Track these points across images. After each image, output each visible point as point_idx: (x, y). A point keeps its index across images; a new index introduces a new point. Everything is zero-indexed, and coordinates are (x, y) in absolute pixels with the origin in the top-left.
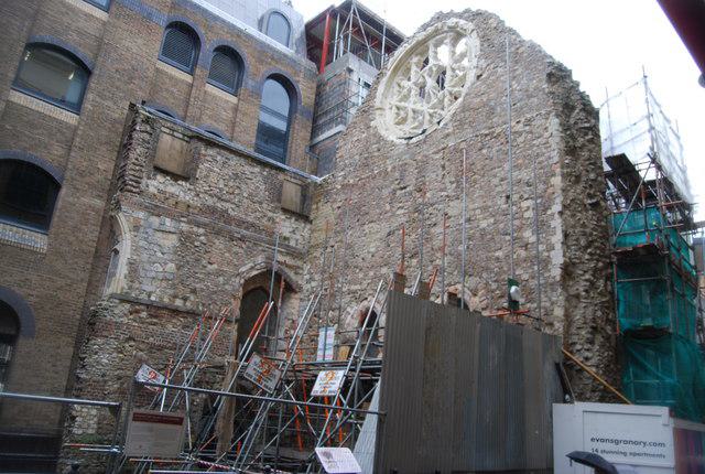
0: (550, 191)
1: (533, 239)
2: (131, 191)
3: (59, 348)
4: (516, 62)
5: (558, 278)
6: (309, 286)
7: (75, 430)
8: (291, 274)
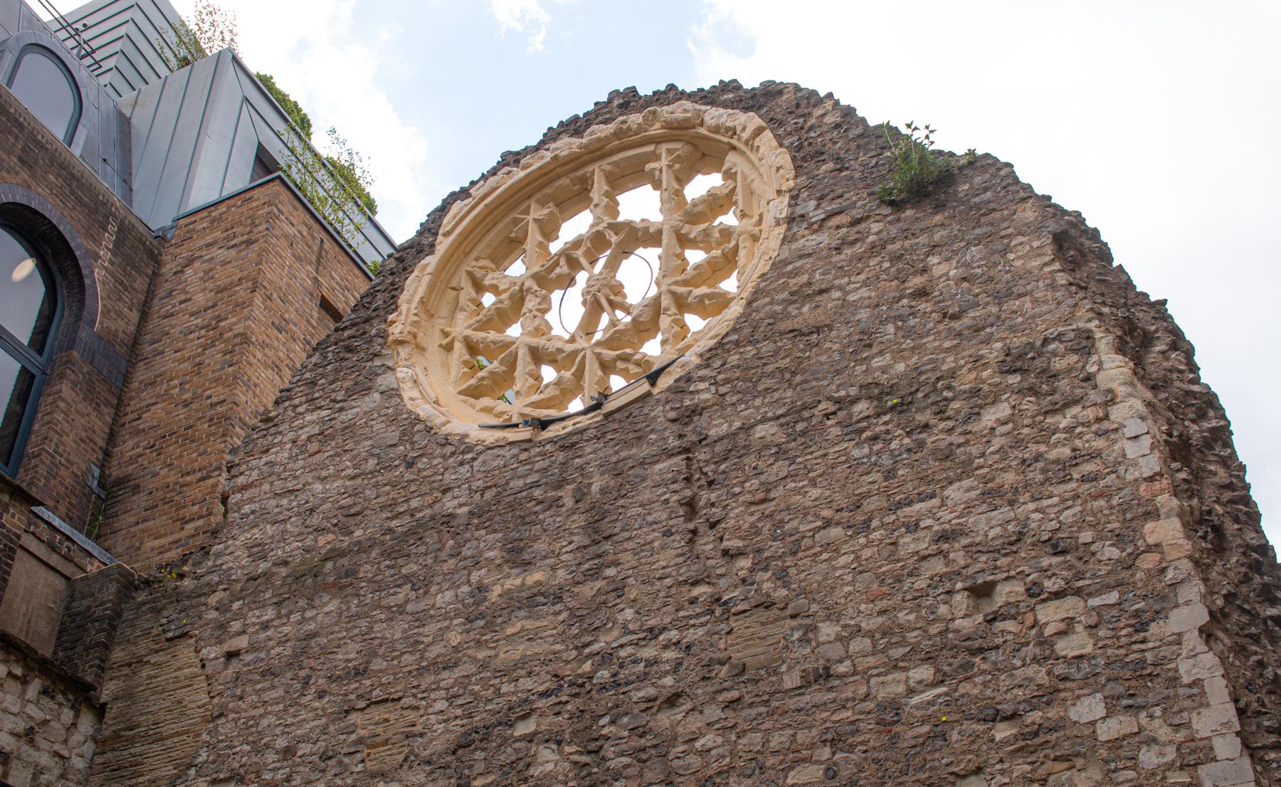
0: (1148, 562)
1: (1109, 729)
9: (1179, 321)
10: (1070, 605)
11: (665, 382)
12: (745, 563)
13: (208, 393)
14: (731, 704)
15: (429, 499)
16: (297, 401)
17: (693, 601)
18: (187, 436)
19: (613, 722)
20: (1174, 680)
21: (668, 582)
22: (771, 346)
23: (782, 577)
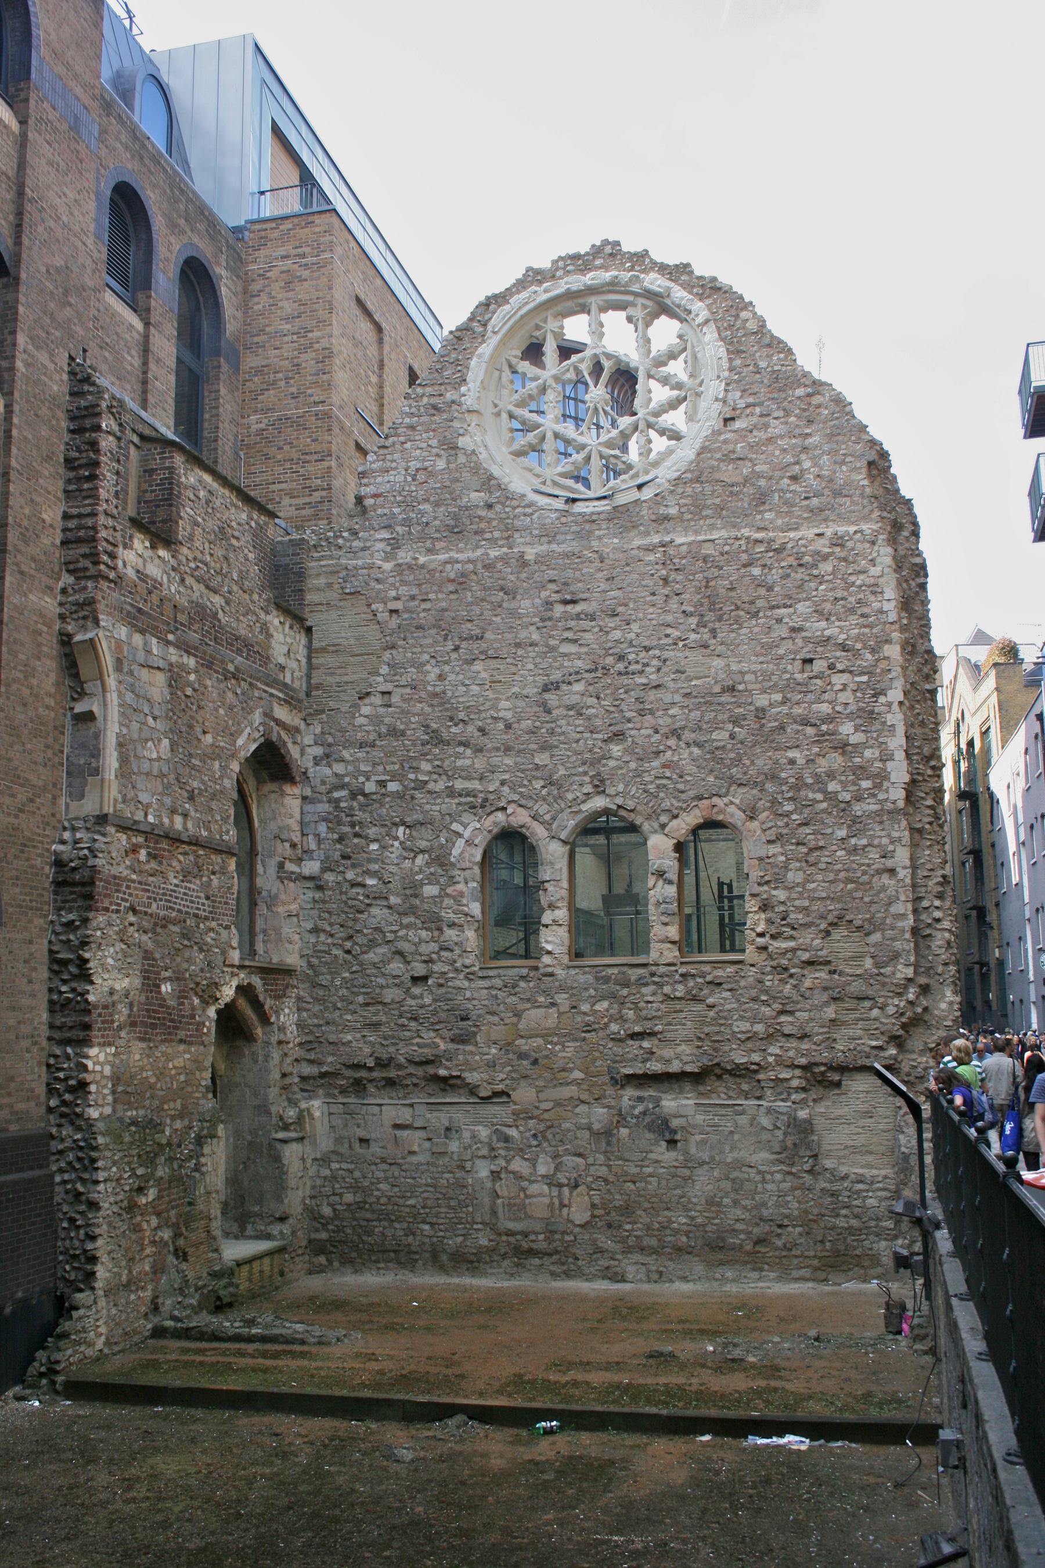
0: (883, 665)
1: (853, 740)
2: (107, 578)
3: (31, 942)
4: (810, 422)
5: (901, 804)
6: (328, 771)
7: (94, 1113)
8: (290, 745)
9: (916, 510)
10: (845, 678)
11: (647, 493)
12: (693, 621)
13: (309, 391)
14: (687, 695)
15: (506, 535)
16: (402, 439)
17: (667, 636)
18: (300, 424)
19: (626, 692)
20: (884, 723)
21: (654, 622)
22: (710, 488)
23: (713, 632)
